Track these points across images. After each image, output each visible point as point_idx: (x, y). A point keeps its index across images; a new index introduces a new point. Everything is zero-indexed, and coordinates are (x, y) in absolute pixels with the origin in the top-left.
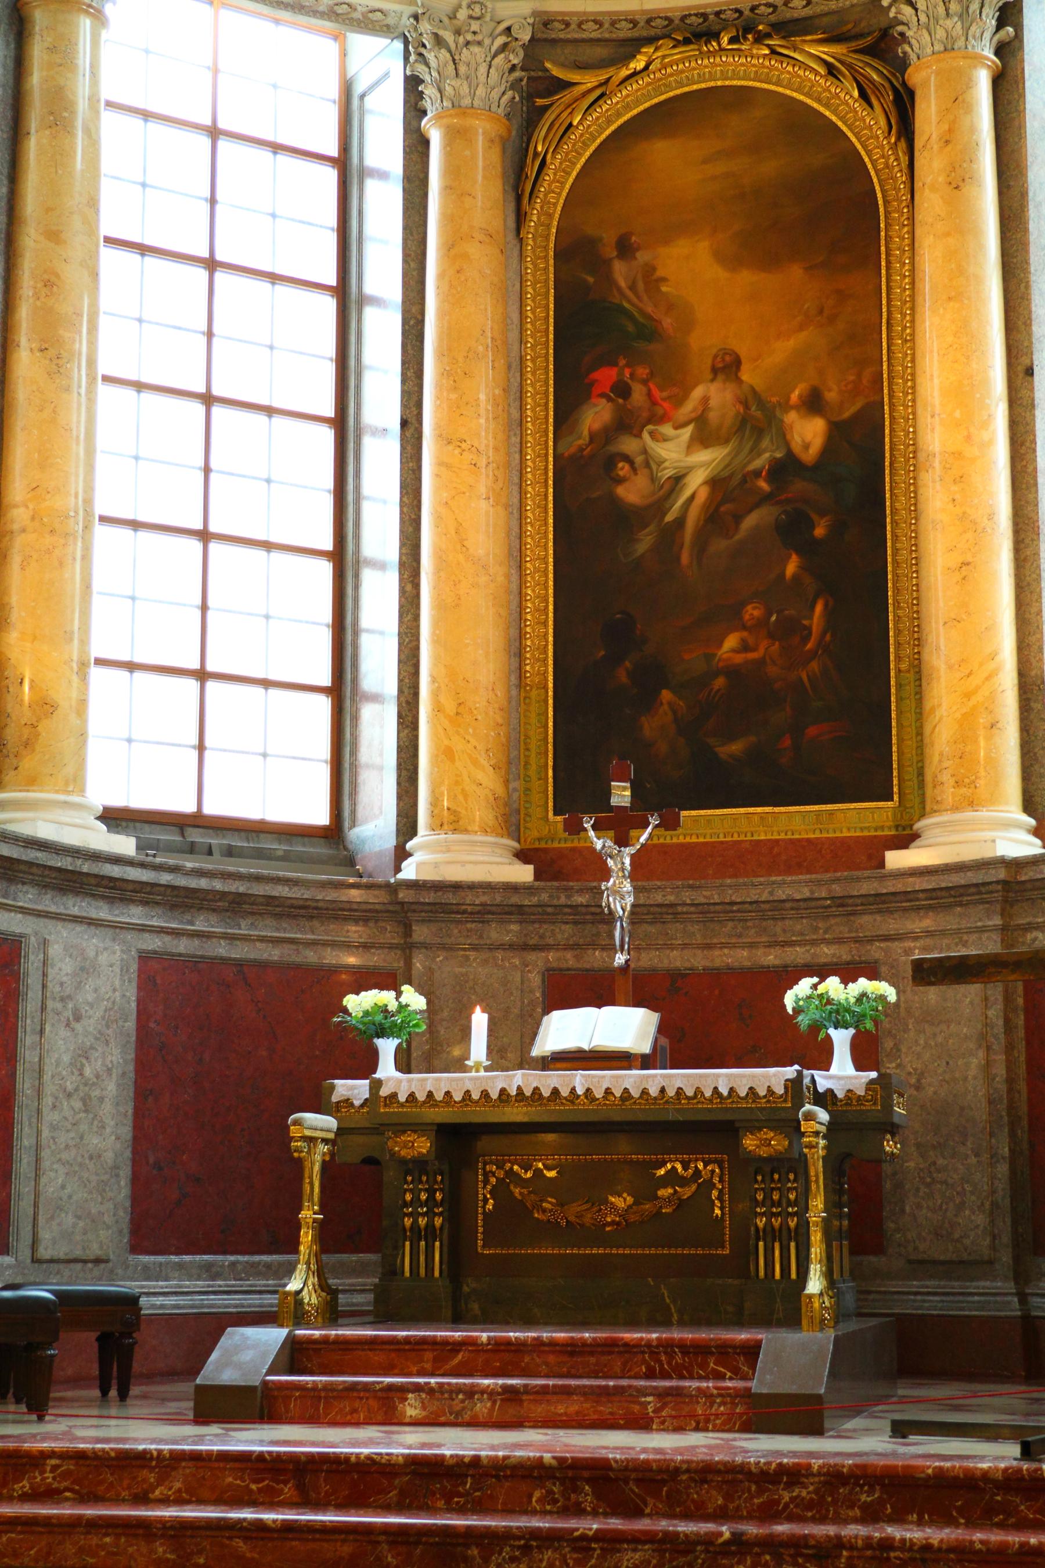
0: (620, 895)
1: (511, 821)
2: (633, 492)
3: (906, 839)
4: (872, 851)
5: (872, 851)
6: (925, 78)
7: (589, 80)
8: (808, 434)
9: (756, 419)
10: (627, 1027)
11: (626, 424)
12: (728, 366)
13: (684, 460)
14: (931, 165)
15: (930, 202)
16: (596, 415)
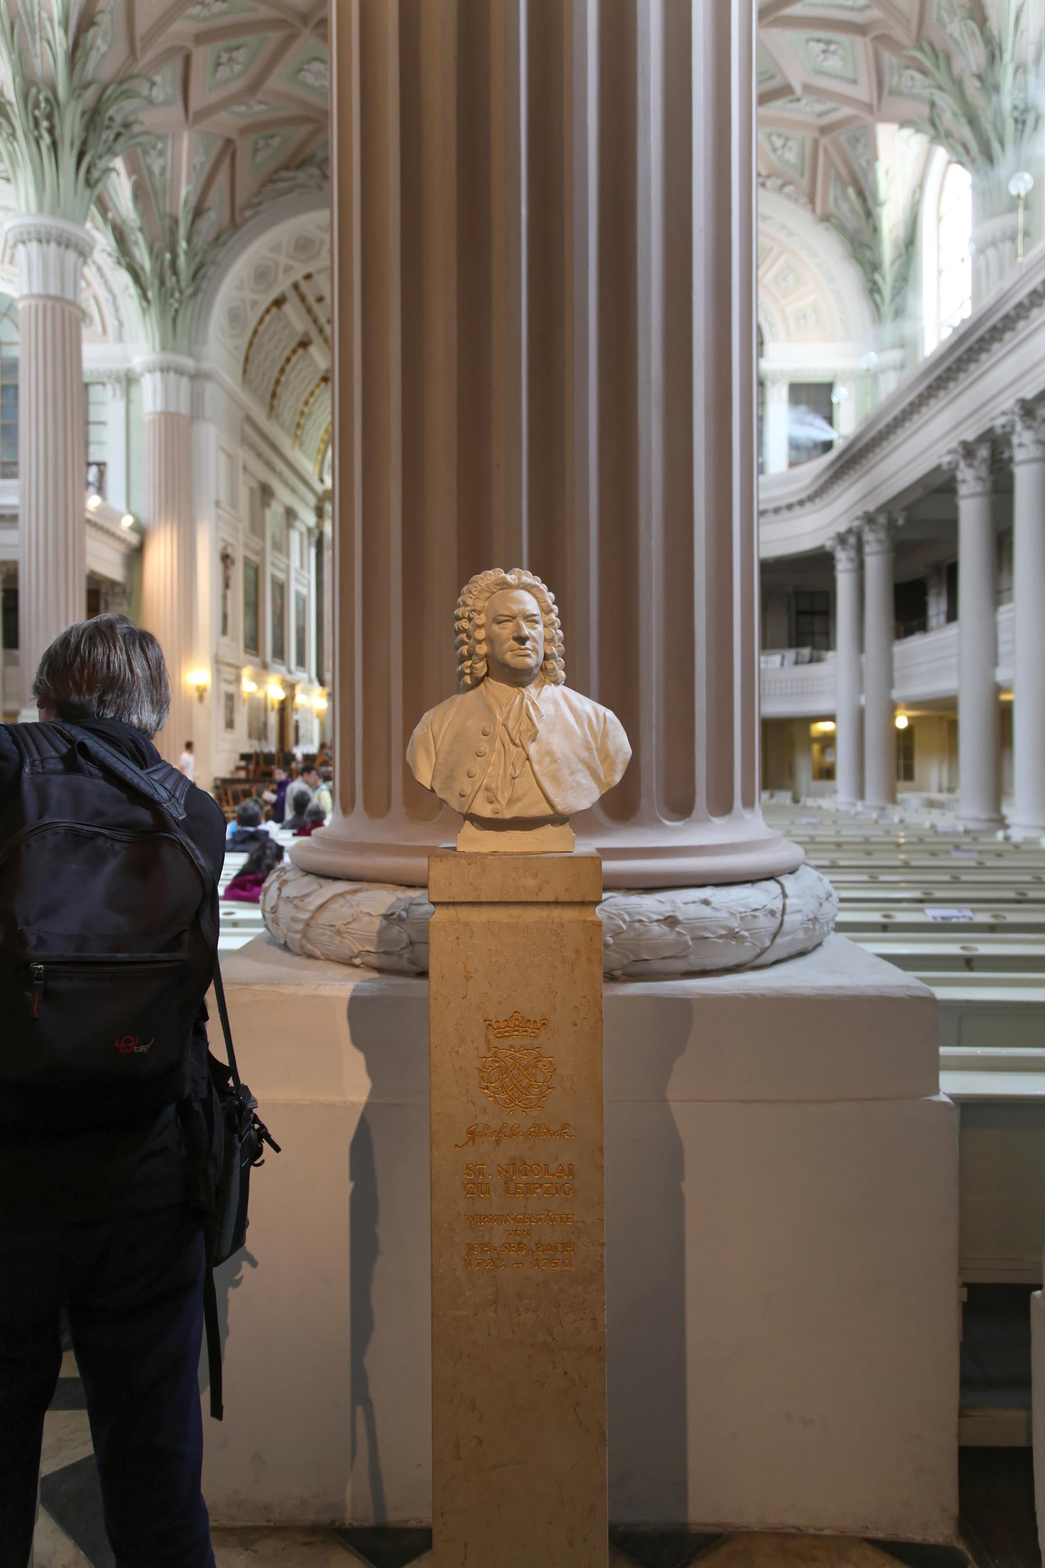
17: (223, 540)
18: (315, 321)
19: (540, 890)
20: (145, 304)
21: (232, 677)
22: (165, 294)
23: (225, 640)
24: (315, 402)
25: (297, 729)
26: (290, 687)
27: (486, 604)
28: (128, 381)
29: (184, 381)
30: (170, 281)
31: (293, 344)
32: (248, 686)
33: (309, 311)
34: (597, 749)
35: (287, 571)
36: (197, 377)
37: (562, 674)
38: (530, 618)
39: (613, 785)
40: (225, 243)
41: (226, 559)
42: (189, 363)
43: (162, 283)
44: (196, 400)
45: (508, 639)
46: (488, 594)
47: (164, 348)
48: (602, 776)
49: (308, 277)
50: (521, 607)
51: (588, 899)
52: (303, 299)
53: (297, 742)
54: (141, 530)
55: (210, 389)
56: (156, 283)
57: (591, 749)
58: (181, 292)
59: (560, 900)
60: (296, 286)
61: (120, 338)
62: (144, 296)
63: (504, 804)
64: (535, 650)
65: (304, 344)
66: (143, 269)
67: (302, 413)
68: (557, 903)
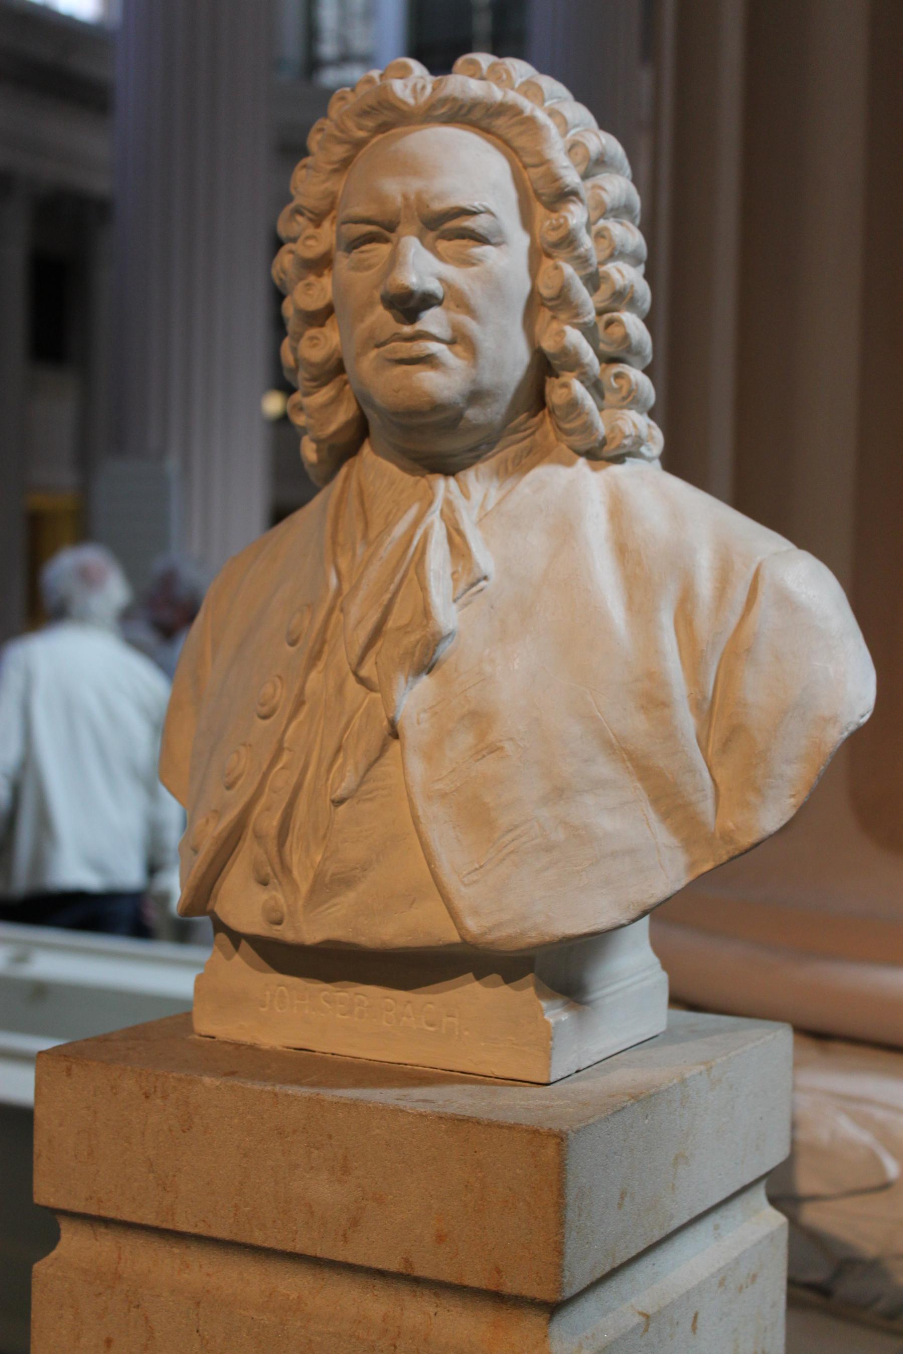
19: (355, 1222)
27: (338, 185)
34: (696, 706)
37: (637, 423)
38: (451, 227)
39: (746, 841)
45: (369, 305)
46: (340, 152)
48: (707, 807)
50: (415, 185)
51: (510, 1286)
57: (665, 704)
59: (419, 1272)
63: (304, 887)
64: (459, 339)
68: (408, 1280)
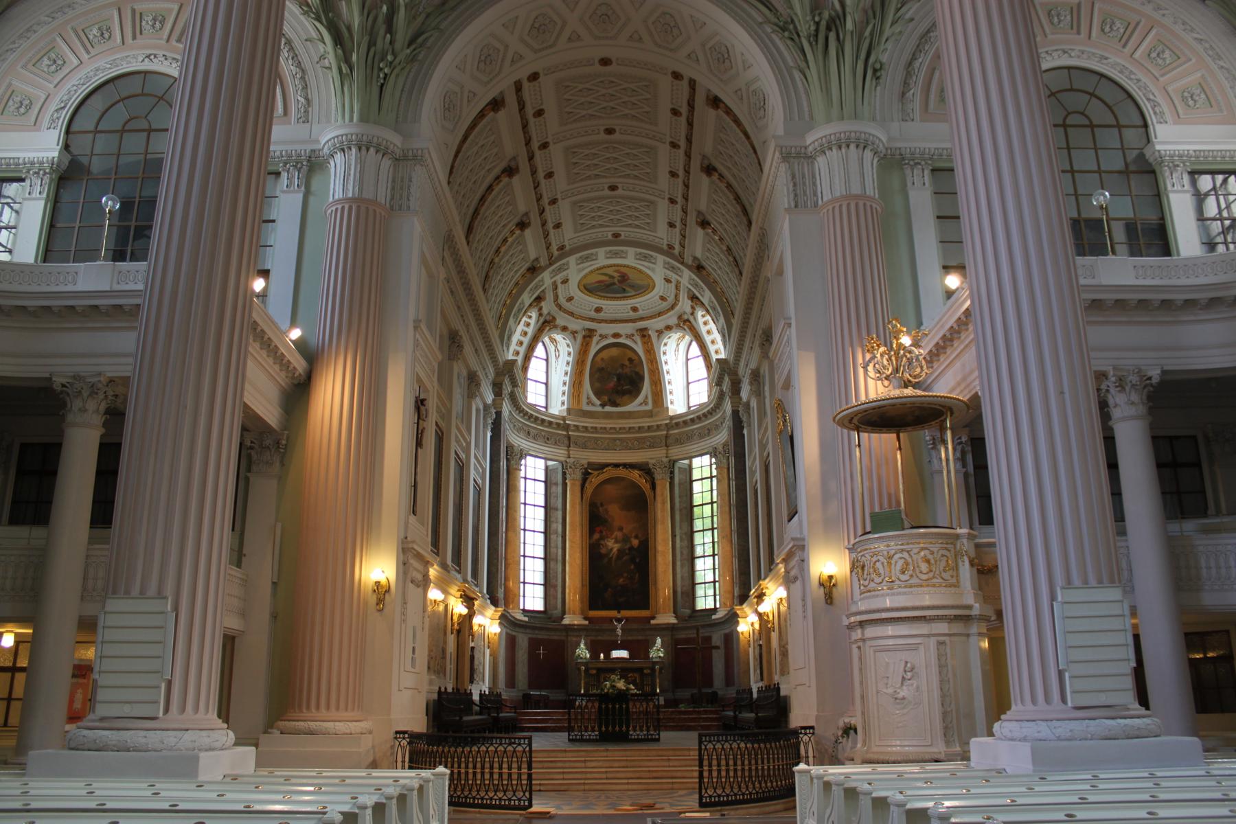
0: (619, 632)
1: (582, 612)
2: (603, 551)
3: (653, 618)
4: (648, 620)
5: (648, 620)
6: (658, 483)
7: (596, 473)
8: (635, 542)
9: (626, 539)
10: (624, 654)
11: (602, 538)
12: (621, 529)
13: (612, 545)
14: (659, 499)
15: (659, 505)
16: (596, 536)
17: (419, 380)
18: (528, 142)
20: (345, 69)
21: (419, 577)
22: (373, 61)
23: (412, 517)
24: (506, 252)
25: (472, 658)
26: (468, 600)
28: (312, 165)
29: (387, 163)
30: (383, 41)
31: (497, 171)
32: (434, 594)
33: (525, 126)
35: (467, 451)
36: (403, 160)
40: (453, 9)
41: (420, 404)
42: (395, 140)
43: (372, 43)
44: (399, 188)
47: (364, 119)
49: (534, 77)
52: (522, 106)
53: (472, 681)
54: (312, 355)
55: (419, 175)
56: (366, 38)
58: (395, 55)
60: (518, 87)
61: (305, 118)
62: (347, 61)
65: (510, 171)
66: (349, 29)
67: (492, 262)
